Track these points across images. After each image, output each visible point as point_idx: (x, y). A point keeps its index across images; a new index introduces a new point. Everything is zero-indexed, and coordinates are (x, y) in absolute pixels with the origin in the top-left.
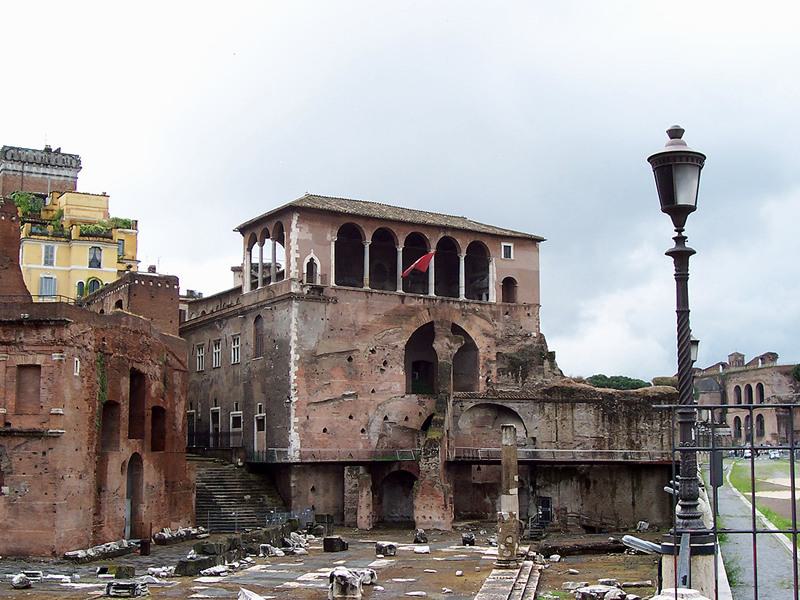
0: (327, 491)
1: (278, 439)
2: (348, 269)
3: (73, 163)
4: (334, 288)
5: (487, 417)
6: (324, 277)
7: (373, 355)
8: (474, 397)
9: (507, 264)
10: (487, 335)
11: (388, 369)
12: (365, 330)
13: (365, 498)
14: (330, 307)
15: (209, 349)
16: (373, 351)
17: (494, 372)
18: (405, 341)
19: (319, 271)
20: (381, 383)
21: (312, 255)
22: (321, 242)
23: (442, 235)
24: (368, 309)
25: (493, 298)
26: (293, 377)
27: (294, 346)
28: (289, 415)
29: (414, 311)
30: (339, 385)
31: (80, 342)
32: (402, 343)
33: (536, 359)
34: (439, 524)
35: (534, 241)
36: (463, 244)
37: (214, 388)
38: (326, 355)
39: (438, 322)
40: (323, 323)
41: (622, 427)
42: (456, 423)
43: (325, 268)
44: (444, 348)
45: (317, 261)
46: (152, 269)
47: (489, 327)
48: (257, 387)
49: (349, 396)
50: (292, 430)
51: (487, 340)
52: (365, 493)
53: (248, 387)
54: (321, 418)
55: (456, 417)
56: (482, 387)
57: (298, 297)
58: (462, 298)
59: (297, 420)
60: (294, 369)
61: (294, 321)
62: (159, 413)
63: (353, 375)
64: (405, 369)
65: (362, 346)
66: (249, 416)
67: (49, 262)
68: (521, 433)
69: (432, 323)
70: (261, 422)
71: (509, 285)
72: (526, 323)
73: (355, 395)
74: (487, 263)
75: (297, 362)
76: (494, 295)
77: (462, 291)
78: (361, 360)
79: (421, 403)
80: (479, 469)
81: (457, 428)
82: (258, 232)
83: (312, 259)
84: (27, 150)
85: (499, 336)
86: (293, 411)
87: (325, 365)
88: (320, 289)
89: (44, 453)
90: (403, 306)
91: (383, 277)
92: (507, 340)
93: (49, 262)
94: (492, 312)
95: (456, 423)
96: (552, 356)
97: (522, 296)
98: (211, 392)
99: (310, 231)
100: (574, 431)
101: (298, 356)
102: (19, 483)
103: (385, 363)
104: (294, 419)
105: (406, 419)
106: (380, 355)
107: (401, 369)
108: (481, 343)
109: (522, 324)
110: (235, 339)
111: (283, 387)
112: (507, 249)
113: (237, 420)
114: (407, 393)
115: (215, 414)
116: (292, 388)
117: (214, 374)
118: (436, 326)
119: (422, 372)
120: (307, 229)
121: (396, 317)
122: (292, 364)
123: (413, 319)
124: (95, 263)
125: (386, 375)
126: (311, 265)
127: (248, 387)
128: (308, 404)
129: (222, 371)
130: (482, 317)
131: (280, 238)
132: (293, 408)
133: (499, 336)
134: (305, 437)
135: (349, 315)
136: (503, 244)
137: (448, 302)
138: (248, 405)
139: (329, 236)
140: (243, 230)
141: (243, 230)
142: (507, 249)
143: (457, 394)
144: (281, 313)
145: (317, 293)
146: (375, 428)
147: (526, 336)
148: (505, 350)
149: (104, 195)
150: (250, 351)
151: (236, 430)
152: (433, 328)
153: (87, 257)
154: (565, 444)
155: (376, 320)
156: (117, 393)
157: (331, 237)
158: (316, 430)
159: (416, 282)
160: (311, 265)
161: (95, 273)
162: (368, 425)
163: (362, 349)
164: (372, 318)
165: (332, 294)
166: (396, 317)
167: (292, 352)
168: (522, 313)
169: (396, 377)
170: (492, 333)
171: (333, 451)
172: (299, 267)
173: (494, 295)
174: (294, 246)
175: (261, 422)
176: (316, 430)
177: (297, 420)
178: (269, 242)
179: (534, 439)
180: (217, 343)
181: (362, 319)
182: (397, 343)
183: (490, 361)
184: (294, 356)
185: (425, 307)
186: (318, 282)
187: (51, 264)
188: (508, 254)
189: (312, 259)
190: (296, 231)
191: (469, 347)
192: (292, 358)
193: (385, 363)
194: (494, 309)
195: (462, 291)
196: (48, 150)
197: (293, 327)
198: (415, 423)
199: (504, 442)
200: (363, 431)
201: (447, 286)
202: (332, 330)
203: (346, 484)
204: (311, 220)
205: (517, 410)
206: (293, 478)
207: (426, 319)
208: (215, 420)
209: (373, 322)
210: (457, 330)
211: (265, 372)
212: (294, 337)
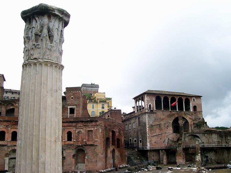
0: (156, 156)
1: (145, 144)
2: (158, 106)
3: (97, 86)
4: (155, 110)
5: (191, 138)
6: (153, 108)
8: (189, 133)
9: (194, 103)
10: (190, 119)
11: (168, 128)
12: (163, 119)
13: (165, 157)
15: (129, 125)
16: (165, 124)
17: (193, 127)
18: (172, 121)
19: (152, 107)
20: (167, 131)
22: (152, 100)
23: (179, 97)
24: (163, 115)
25: (191, 111)
26: (147, 131)
27: (147, 124)
28: (147, 139)
29: (174, 114)
30: (158, 132)
31: (101, 125)
32: (171, 122)
33: (202, 124)
34: (182, 163)
35: (200, 97)
36: (184, 99)
37: (130, 134)
38: (154, 125)
41: (224, 139)
42: (185, 139)
43: (153, 106)
44: (181, 122)
45: (151, 104)
46: (115, 108)
47: (191, 117)
48: (139, 133)
49: (160, 134)
51: (190, 120)
52: (165, 156)
53: (137, 133)
54: (154, 139)
55: (185, 138)
56: (190, 131)
57: (147, 113)
58: (184, 111)
59: (149, 140)
60: (147, 129)
61: (147, 118)
62: (118, 140)
63: (161, 129)
64: (172, 128)
65: (162, 123)
66: (138, 140)
67: (93, 108)
68: (200, 141)
69: (178, 117)
70: (141, 141)
71: (195, 107)
72: (199, 116)
73: (161, 134)
74: (190, 102)
75: (148, 127)
76: (192, 110)
77: (184, 109)
78: (162, 126)
79: (176, 135)
80: (191, 150)
81: (185, 140)
82: (138, 99)
83: (150, 104)
84: (87, 84)
85: (193, 119)
86: (148, 138)
87: (154, 127)
88: (152, 111)
89: (94, 149)
90: (171, 114)
91: (166, 107)
92: (195, 120)
93: (93, 108)
94: (192, 114)
95: (185, 139)
96: (206, 123)
97: (198, 110)
98: (129, 135)
99: (149, 98)
100: (212, 140)
102: (89, 156)
103: (168, 127)
104: (148, 140)
105: (173, 139)
108: (189, 121)
110: (134, 123)
111: (145, 133)
112: (194, 99)
113: (135, 141)
114: (173, 133)
115: (130, 139)
117: (130, 131)
118: (179, 118)
119: (176, 128)
120: (149, 98)
121: (170, 116)
122: (147, 128)
123: (174, 116)
124: (103, 108)
125: (168, 129)
127: (137, 133)
128: (151, 137)
129: (132, 130)
130: (189, 115)
131: (143, 100)
132: (148, 137)
133: (193, 119)
134: (151, 144)
136: (193, 98)
137: (181, 112)
138: (138, 137)
140: (134, 99)
141: (134, 99)
142: (194, 99)
143: (185, 133)
144: (144, 116)
145: (152, 112)
146: (166, 141)
147: (200, 119)
148: (195, 122)
149: (104, 93)
150: (138, 125)
151: (135, 143)
152: (178, 118)
153: (101, 106)
154: (210, 143)
155: (165, 117)
156: (109, 136)
157: (154, 99)
158: (153, 142)
159: (174, 108)
161: (103, 110)
162: (165, 140)
163: (162, 124)
164: (164, 117)
165: (155, 112)
166: (170, 116)
167: (147, 125)
168: (198, 113)
169: (170, 130)
171: (157, 147)
172: (147, 106)
173: (192, 110)
174: (146, 102)
175: (141, 141)
176: (153, 142)
177: (149, 140)
178: (140, 101)
179: (203, 142)
180: (130, 124)
181: (162, 117)
182: (170, 122)
183: (192, 125)
184: (147, 126)
185: (176, 113)
186: (152, 109)
187: (94, 108)
188: (194, 100)
189: (150, 104)
190: (146, 98)
191: (187, 122)
192: (147, 126)
193: (168, 127)
194: (192, 113)
195: (184, 109)
196: (92, 84)
197: (147, 119)
198: (175, 140)
199: (196, 143)
200: (164, 142)
201: (181, 108)
202: (155, 120)
203: (160, 154)
204: (150, 96)
205: (198, 136)
206: (148, 153)
207: (176, 116)
208: (131, 141)
210: (183, 118)
211: (141, 130)
212: (147, 122)
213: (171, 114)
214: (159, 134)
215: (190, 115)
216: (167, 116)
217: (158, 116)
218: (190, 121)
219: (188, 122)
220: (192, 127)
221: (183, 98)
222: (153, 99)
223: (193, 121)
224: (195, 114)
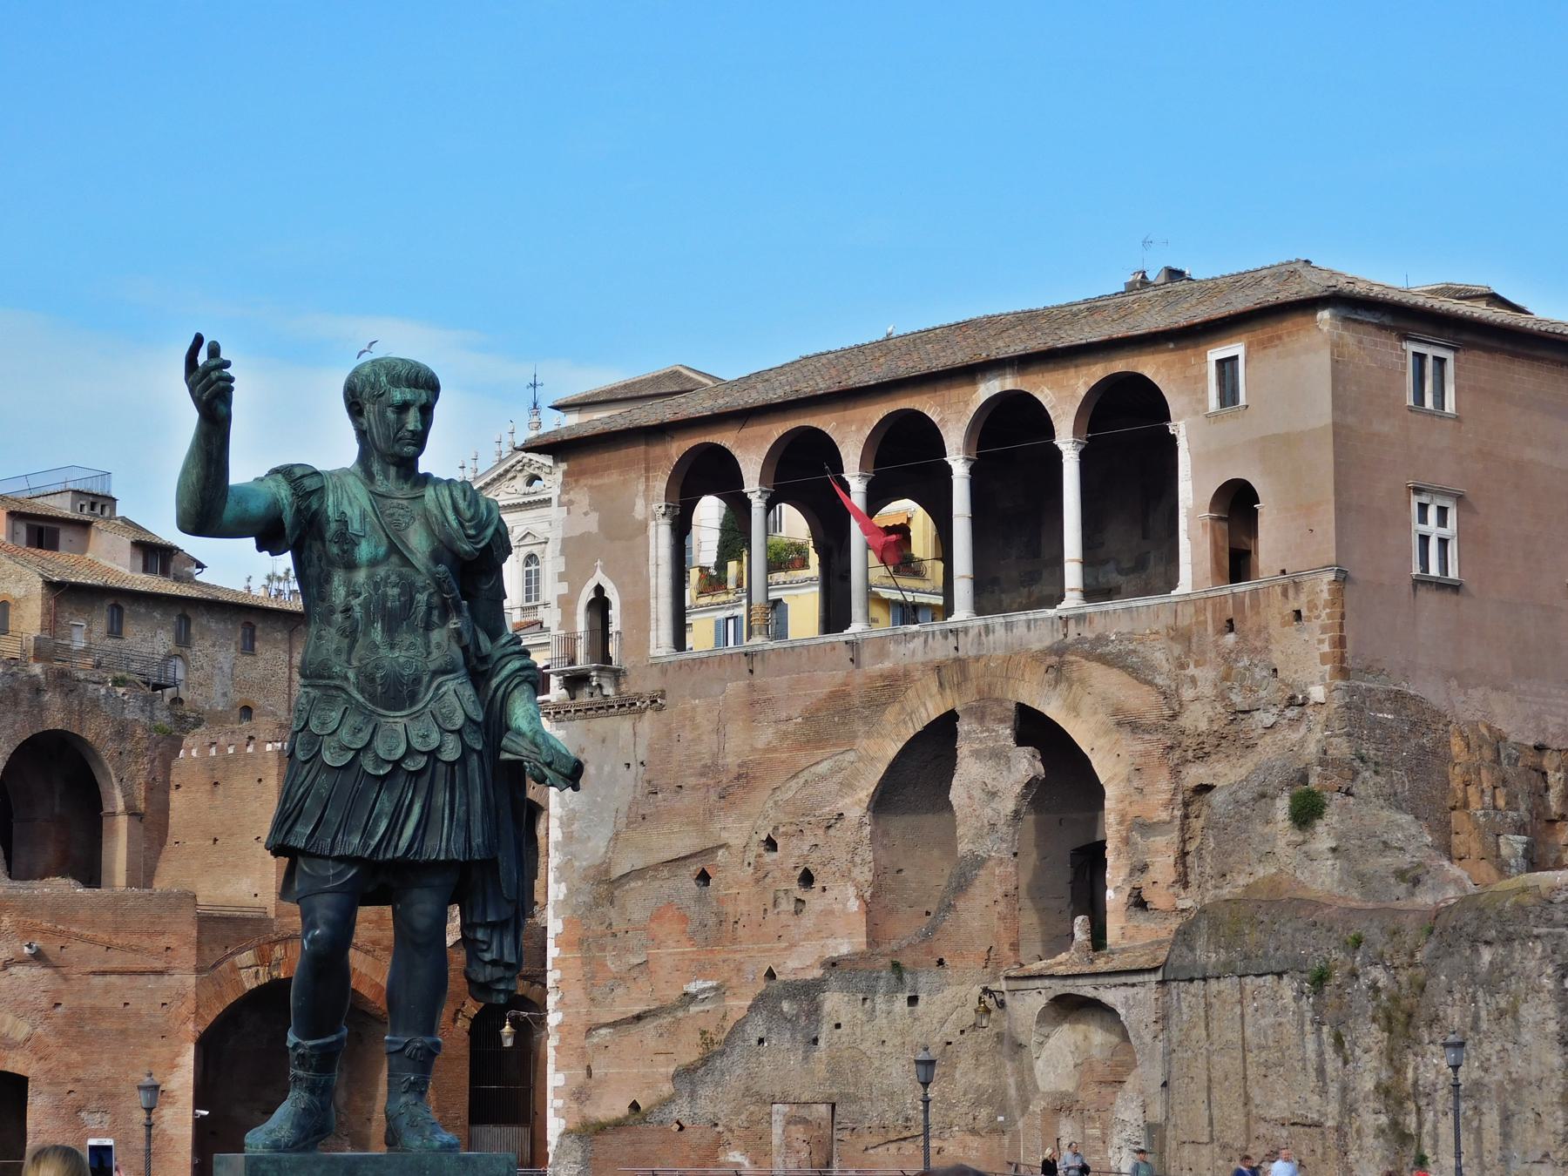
7: (770, 857)
11: (812, 897)
12: (745, 778)
14: (648, 723)
16: (771, 844)
17: (1163, 866)
18: (865, 790)
21: (599, 577)
29: (893, 686)
39: (969, 710)
40: (629, 776)
45: (611, 593)
47: (1138, 699)
50: (550, 1113)
51: (1133, 746)
58: (1072, 600)
65: (737, 832)
77: (1073, 574)
78: (732, 875)
83: (599, 590)
87: (637, 903)
99: (595, 506)
101: (563, 887)
103: (807, 879)
104: (555, 1079)
106: (791, 854)
107: (852, 891)
109: (1277, 658)
116: (550, 983)
118: (963, 727)
123: (891, 714)
125: (808, 920)
126: (600, 604)
133: (1198, 717)
135: (697, 740)
136: (1216, 353)
139: (640, 505)
152: (953, 734)
160: (600, 604)
163: (735, 838)
164: (765, 735)
168: (1275, 611)
170: (1151, 717)
181: (739, 745)
182: (841, 804)
183: (1146, 827)
189: (599, 590)
193: (807, 879)
194: (1186, 618)
195: (1073, 574)
207: (931, 710)
209: (770, 749)
213: (859, 678)
214: (689, 998)
215: (1139, 672)
216: (810, 717)
217: (687, 735)
218: (1123, 770)
219: (1097, 792)
220: (1144, 868)
223: (1202, 756)
224: (1230, 626)
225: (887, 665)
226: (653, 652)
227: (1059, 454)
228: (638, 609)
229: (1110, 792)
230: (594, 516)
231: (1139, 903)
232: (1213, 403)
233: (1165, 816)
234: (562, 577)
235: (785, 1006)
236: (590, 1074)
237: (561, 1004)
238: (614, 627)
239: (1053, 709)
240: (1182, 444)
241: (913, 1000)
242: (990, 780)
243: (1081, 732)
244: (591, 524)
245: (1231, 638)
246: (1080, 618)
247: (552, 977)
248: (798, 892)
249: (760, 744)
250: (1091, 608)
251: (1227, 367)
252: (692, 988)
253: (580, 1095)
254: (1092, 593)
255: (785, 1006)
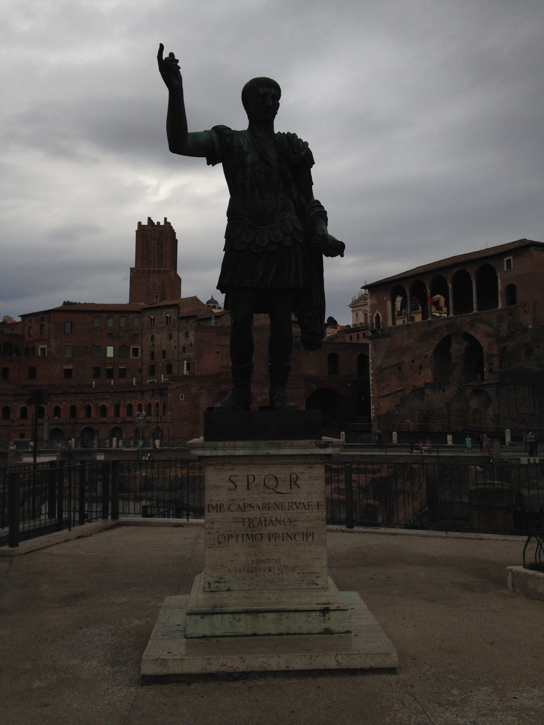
16: (413, 362)
27: (371, 366)
32: (430, 353)
36: (472, 272)
49: (401, 391)
77: (475, 306)
83: (377, 314)
104: (372, 407)
108: (484, 343)
112: (509, 262)
126: (378, 317)
136: (505, 259)
147: (525, 330)
160: (378, 317)
184: (371, 371)
189: (377, 314)
193: (421, 368)
195: (475, 306)
207: (446, 334)
219: (481, 349)
221: (469, 270)
222: (385, 299)
224: (510, 314)
225: (436, 326)
226: (389, 325)
227: (472, 282)
228: (385, 317)
229: (484, 349)
230: (376, 300)
231: (491, 371)
232: (505, 269)
233: (496, 353)
234: (370, 312)
235: (417, 392)
236: (379, 405)
237: (373, 393)
238: (381, 321)
239: (472, 333)
240: (499, 278)
241: (444, 391)
242: (457, 348)
243: (478, 337)
244: (376, 302)
245: (510, 317)
246: (477, 314)
247: (371, 388)
248: (419, 371)
249: (411, 342)
250: (479, 312)
251: (509, 262)
252: (398, 389)
253: (377, 409)
254: (479, 309)
255: (417, 392)
